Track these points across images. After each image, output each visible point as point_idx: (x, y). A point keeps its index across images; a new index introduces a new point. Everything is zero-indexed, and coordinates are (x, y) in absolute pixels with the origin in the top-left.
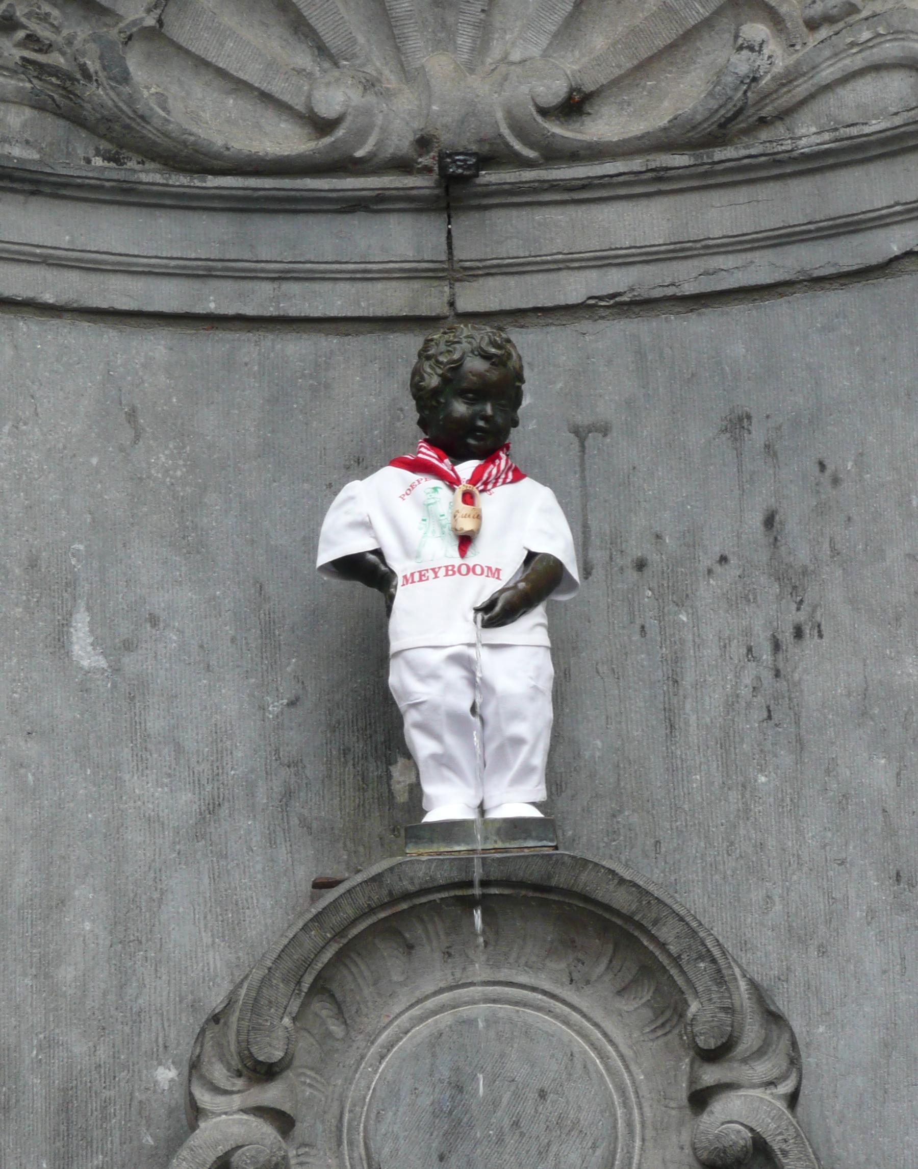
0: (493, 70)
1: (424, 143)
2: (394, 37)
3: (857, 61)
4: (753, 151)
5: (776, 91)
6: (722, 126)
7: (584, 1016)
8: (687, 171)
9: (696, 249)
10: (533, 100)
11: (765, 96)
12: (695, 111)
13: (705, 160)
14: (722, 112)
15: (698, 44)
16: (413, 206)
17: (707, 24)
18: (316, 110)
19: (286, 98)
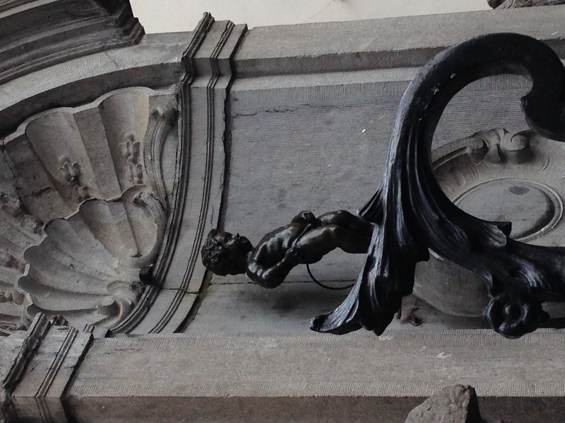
0: (118, 273)
1: (134, 287)
2: (94, 294)
3: (157, 162)
4: (175, 194)
5: (158, 192)
6: (164, 210)
7: (465, 193)
8: (175, 218)
9: (202, 223)
10: (133, 257)
11: (158, 194)
12: (155, 215)
13: (173, 210)
14: (159, 207)
15: (134, 220)
16: (155, 294)
17: (128, 214)
18: (109, 304)
19: (101, 319)
